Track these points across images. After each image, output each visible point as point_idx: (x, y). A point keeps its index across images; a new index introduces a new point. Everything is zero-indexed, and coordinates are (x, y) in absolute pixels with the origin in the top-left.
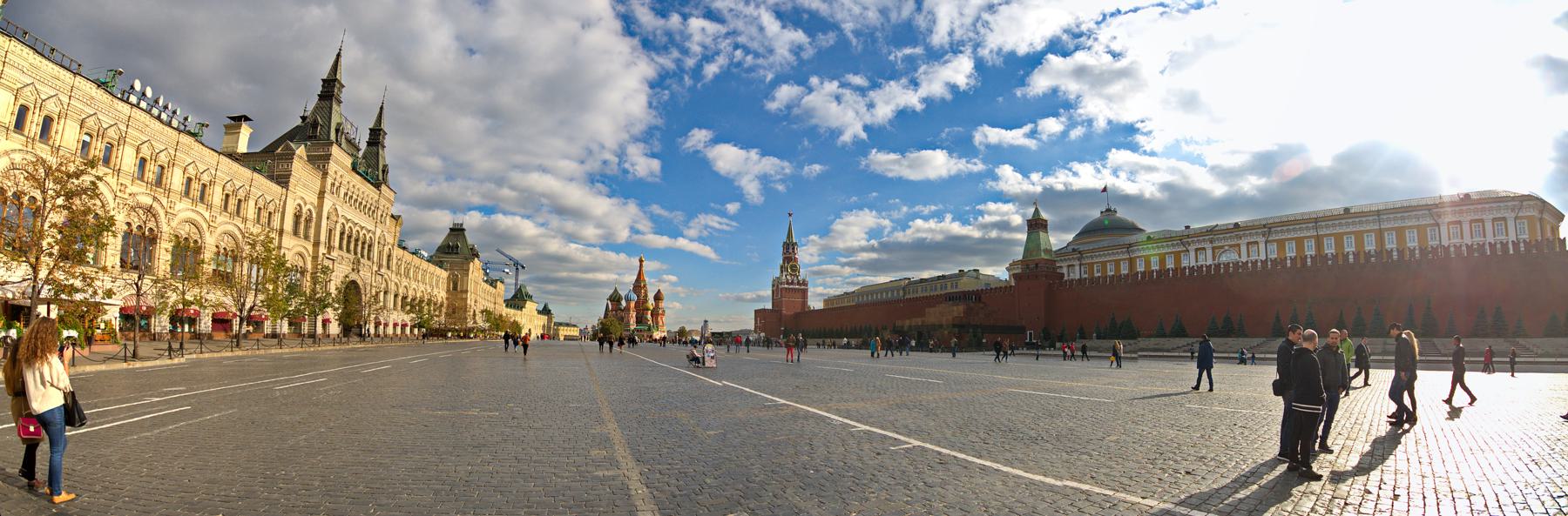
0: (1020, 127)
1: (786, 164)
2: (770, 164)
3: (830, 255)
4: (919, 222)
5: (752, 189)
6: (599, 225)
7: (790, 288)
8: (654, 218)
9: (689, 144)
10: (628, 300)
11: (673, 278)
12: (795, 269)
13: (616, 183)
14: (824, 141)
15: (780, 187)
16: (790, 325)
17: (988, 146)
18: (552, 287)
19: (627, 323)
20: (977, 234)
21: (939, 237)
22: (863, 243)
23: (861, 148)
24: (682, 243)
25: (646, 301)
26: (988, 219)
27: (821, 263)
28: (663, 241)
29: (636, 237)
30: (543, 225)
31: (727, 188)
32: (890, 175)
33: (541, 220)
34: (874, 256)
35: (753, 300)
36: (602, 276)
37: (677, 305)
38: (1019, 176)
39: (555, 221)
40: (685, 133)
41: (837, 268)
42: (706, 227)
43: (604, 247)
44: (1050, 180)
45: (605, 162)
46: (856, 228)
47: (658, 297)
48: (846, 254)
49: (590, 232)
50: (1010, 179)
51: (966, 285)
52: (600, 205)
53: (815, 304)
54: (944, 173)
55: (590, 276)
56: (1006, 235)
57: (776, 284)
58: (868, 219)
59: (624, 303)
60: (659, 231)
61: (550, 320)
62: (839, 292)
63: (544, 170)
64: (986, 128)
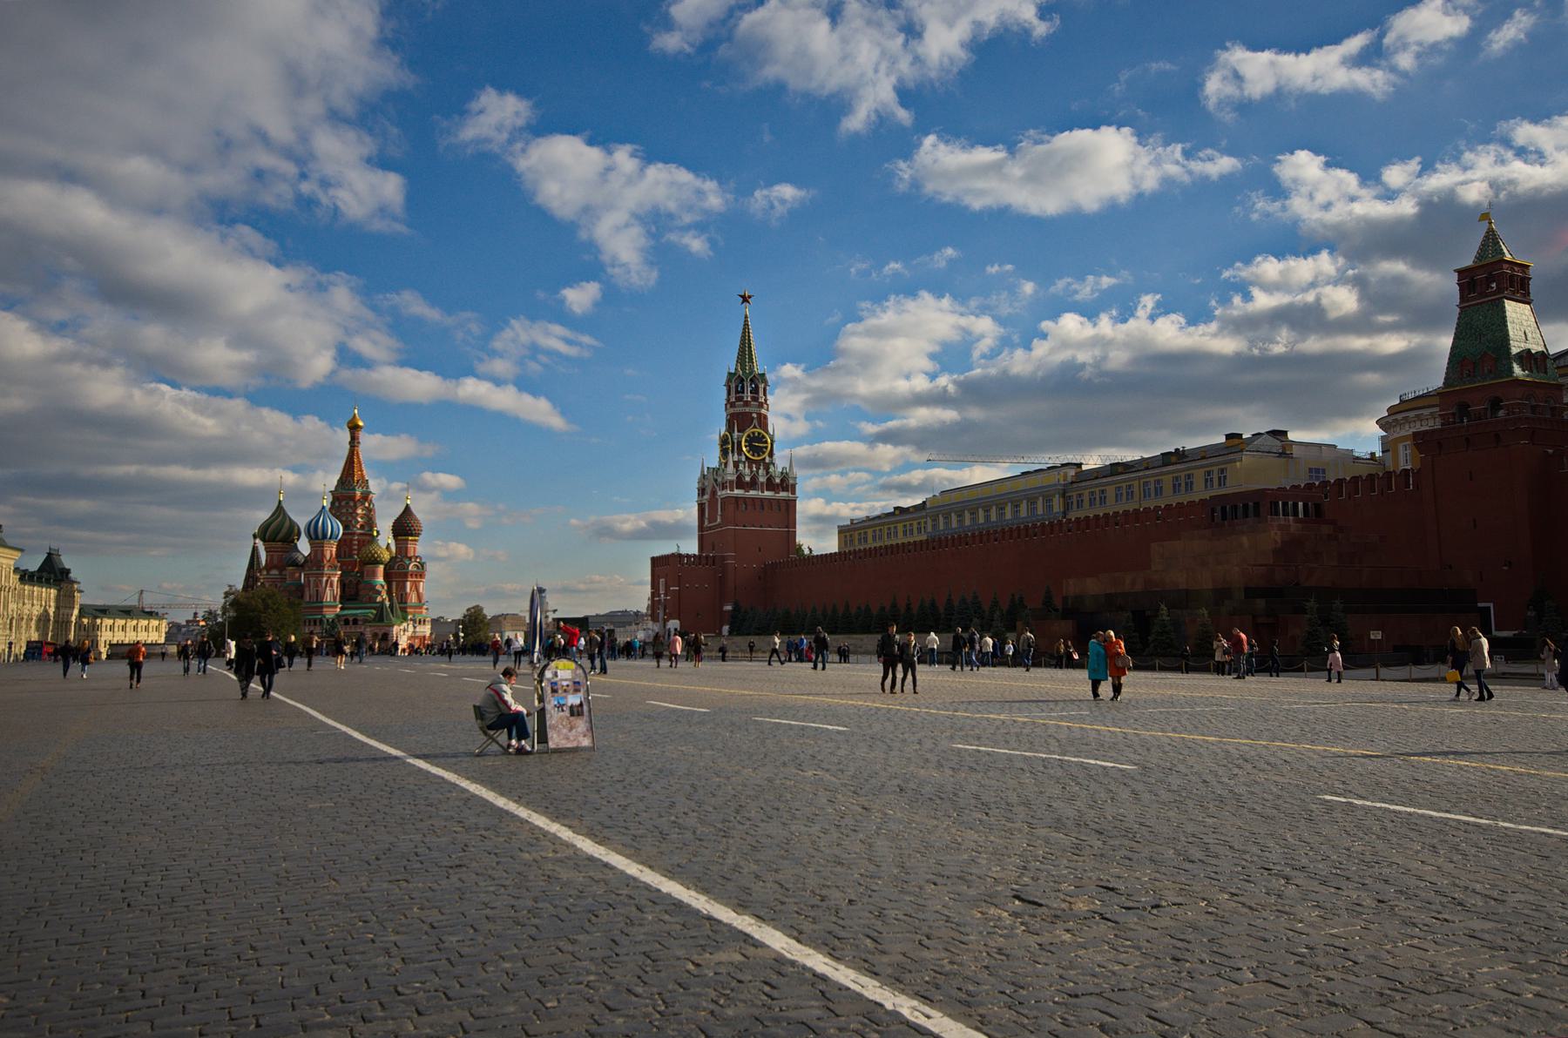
7: (746, 501)
10: (317, 536)
12: (760, 445)
19: (303, 603)
25: (369, 537)
37: (462, 549)
47: (405, 527)
51: (1247, 476)
53: (817, 541)
57: (709, 487)
59: (304, 547)
62: (883, 504)
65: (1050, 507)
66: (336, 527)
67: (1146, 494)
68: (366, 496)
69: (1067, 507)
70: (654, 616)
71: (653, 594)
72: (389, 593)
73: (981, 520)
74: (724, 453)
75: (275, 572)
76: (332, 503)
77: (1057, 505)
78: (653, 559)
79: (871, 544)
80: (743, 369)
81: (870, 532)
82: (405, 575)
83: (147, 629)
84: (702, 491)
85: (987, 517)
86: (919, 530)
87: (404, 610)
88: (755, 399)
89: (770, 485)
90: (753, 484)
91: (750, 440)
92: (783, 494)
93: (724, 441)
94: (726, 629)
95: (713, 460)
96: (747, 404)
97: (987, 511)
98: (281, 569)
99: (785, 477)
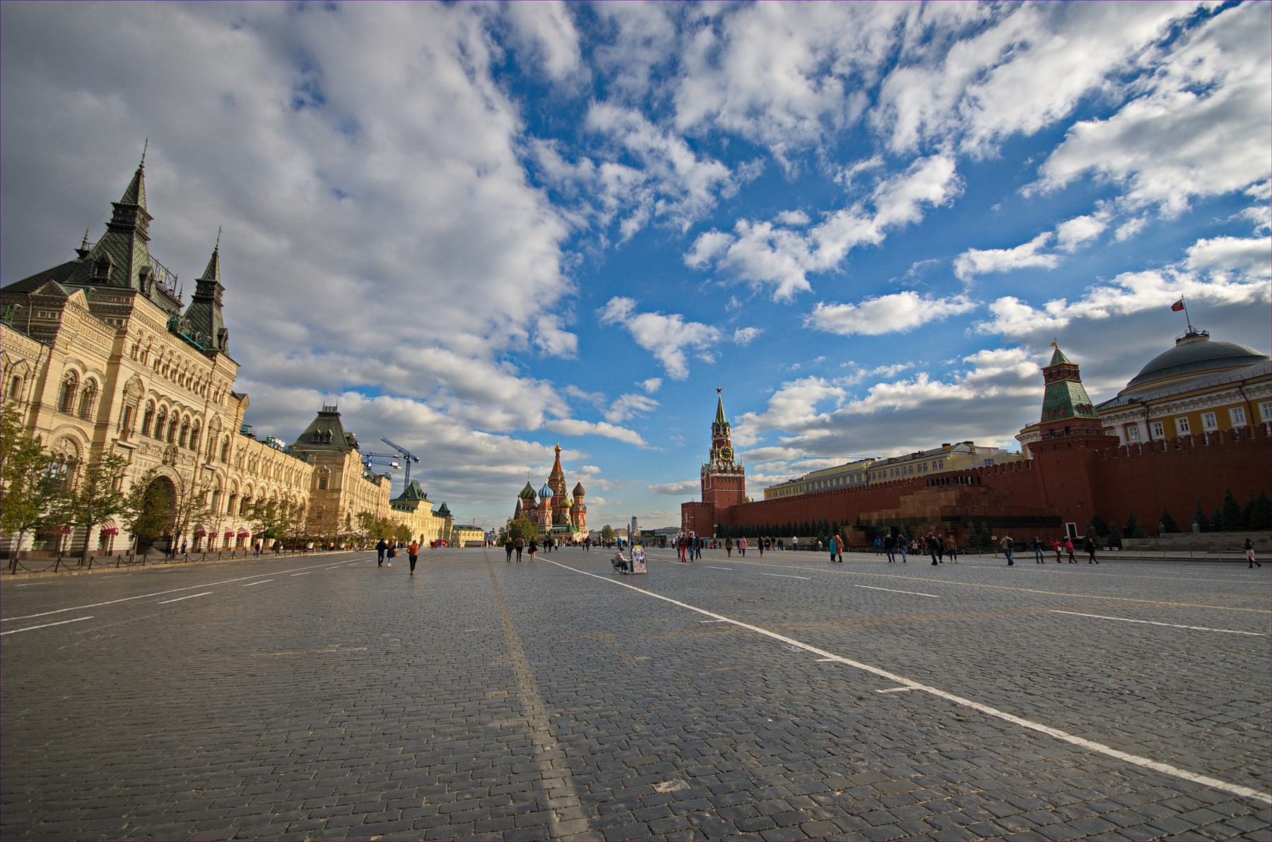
0: (1027, 239)
1: (713, 330)
2: (694, 332)
3: (770, 434)
4: (882, 387)
5: (674, 362)
6: (508, 410)
7: (723, 478)
8: (571, 401)
9: (609, 315)
10: (543, 497)
11: (595, 469)
12: (727, 453)
13: (526, 361)
14: (757, 299)
15: (708, 358)
16: (724, 519)
17: (977, 277)
18: (451, 483)
19: (537, 527)
20: (967, 394)
21: (913, 404)
22: (811, 418)
23: (804, 301)
24: (603, 428)
25: (564, 497)
26: (980, 373)
27: (759, 445)
28: (582, 427)
29: (551, 423)
30: (440, 410)
31: (649, 363)
32: (842, 332)
33: (438, 404)
34: (826, 433)
35: (680, 492)
36: (512, 469)
37: (601, 500)
38: (1028, 310)
39: (456, 406)
40: (603, 302)
41: (779, 450)
42: (631, 409)
43: (513, 436)
44: (1080, 308)
45: (513, 337)
46: (799, 402)
47: (578, 492)
48: (790, 433)
49: (498, 418)
50: (1014, 314)
51: (953, 463)
52: (509, 387)
53: (755, 494)
54: (914, 321)
55: (498, 469)
56: (1013, 392)
57: (706, 474)
58: (815, 388)
59: (538, 500)
60: (577, 416)
61: (448, 523)
62: (783, 479)
63: (440, 345)
64: (974, 254)
66: (550, 492)
67: (905, 473)
68: (562, 479)
70: (683, 529)
74: (712, 457)
77: (864, 478)
84: (703, 474)
89: (733, 471)
90: (725, 471)
91: (723, 452)
93: (712, 452)
99: (739, 467)
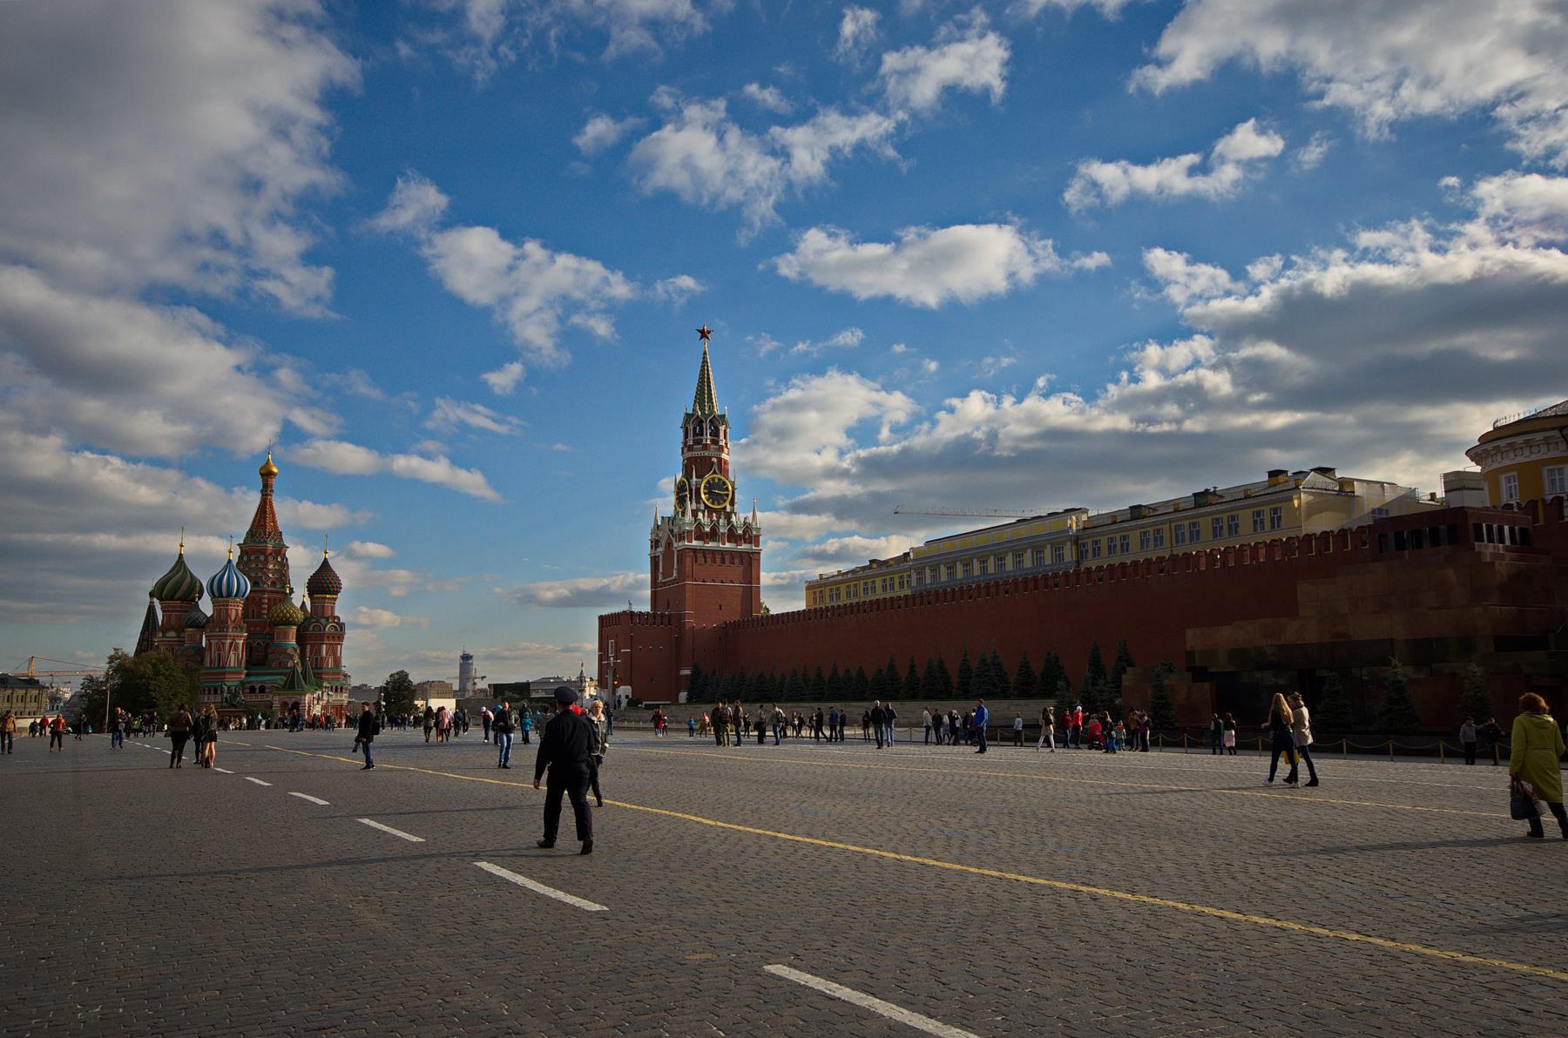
7: (704, 548)
12: (720, 493)
25: (284, 596)
47: (323, 583)
59: (206, 606)
65: (1060, 557)
69: (1081, 555)
71: (601, 659)
72: (302, 656)
73: (977, 572)
74: (681, 501)
75: (172, 634)
76: (240, 558)
77: (1069, 553)
78: (601, 618)
79: (844, 601)
80: (702, 409)
81: (843, 588)
82: (321, 637)
83: (23, 699)
84: (655, 543)
85: (984, 569)
86: (901, 585)
87: (319, 676)
88: (715, 442)
89: (732, 536)
90: (714, 535)
91: (710, 487)
92: (744, 547)
93: (680, 488)
94: (683, 696)
95: (666, 506)
96: (706, 447)
97: (983, 562)
98: (180, 630)
99: (747, 527)
